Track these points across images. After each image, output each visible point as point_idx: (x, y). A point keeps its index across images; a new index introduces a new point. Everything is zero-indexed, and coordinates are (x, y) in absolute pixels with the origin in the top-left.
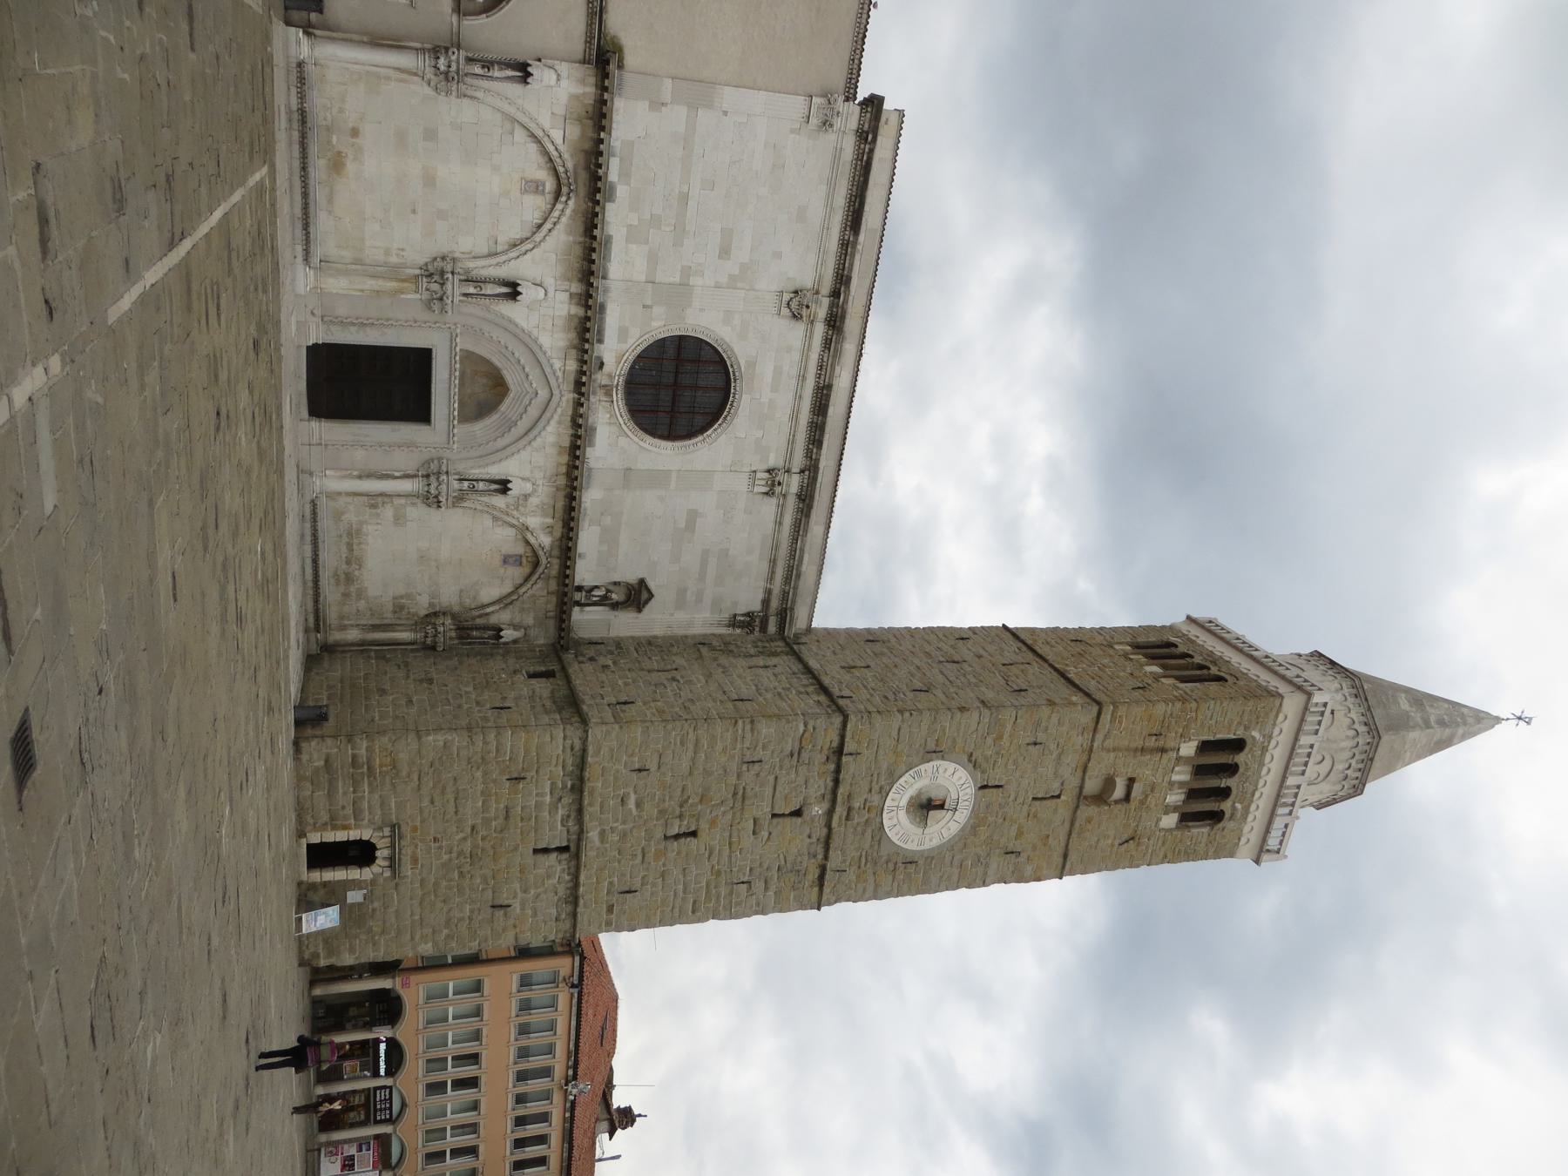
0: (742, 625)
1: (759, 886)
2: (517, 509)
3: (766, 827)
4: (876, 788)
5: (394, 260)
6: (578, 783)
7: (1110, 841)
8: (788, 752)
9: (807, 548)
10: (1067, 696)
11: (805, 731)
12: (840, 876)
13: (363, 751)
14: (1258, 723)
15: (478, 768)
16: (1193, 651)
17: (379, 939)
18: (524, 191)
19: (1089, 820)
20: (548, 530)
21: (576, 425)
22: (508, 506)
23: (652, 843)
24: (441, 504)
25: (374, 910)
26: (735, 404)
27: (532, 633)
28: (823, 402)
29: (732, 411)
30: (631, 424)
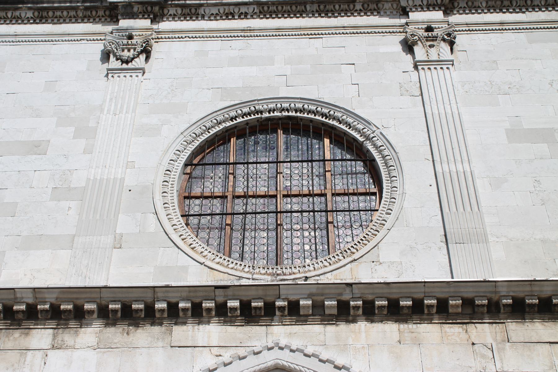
26: (300, 106)
29: (313, 108)
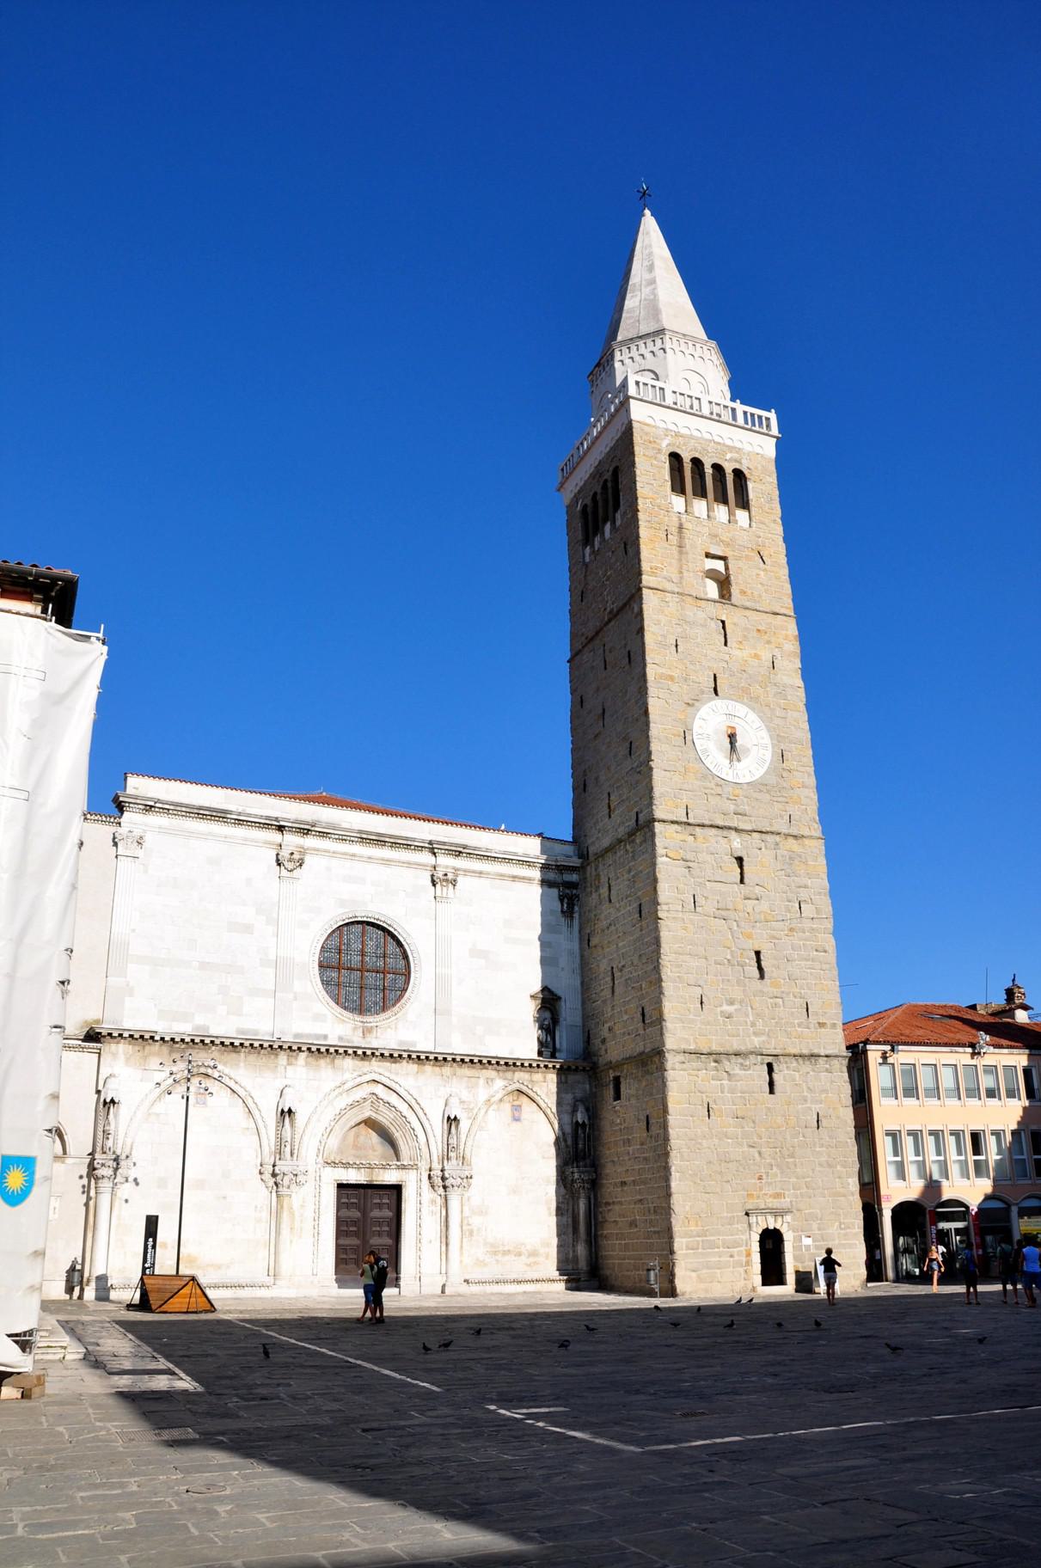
0: (571, 906)
1: (804, 895)
2: (472, 1109)
3: (751, 889)
4: (719, 790)
5: (265, 1215)
6: (712, 1058)
7: (762, 573)
8: (687, 870)
9: (503, 849)
10: (634, 616)
11: (667, 856)
12: (794, 820)
14: (655, 442)
15: (700, 1144)
16: (591, 491)
17: (844, 1223)
19: (743, 592)
20: (490, 1082)
22: (470, 1118)
23: (765, 990)
25: (819, 1229)
26: (377, 917)
27: (579, 1095)
29: (383, 919)
30: (396, 1009)
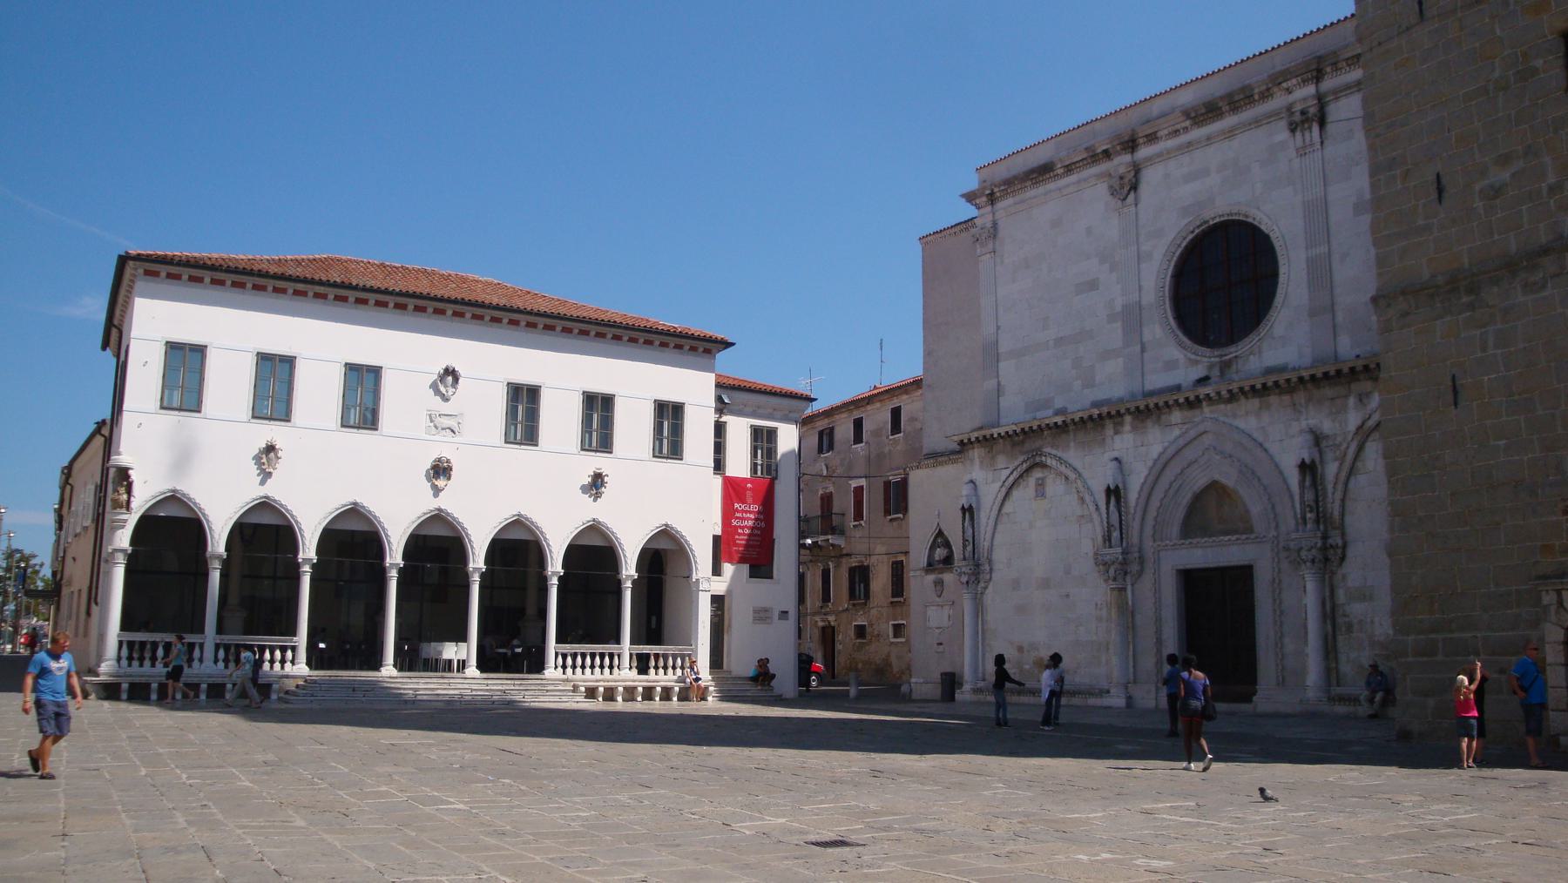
5: (1104, 612)
13: (1411, 638)
18: (1043, 495)
21: (1232, 397)
22: (1336, 460)
24: (1334, 544)
28: (1203, 111)
